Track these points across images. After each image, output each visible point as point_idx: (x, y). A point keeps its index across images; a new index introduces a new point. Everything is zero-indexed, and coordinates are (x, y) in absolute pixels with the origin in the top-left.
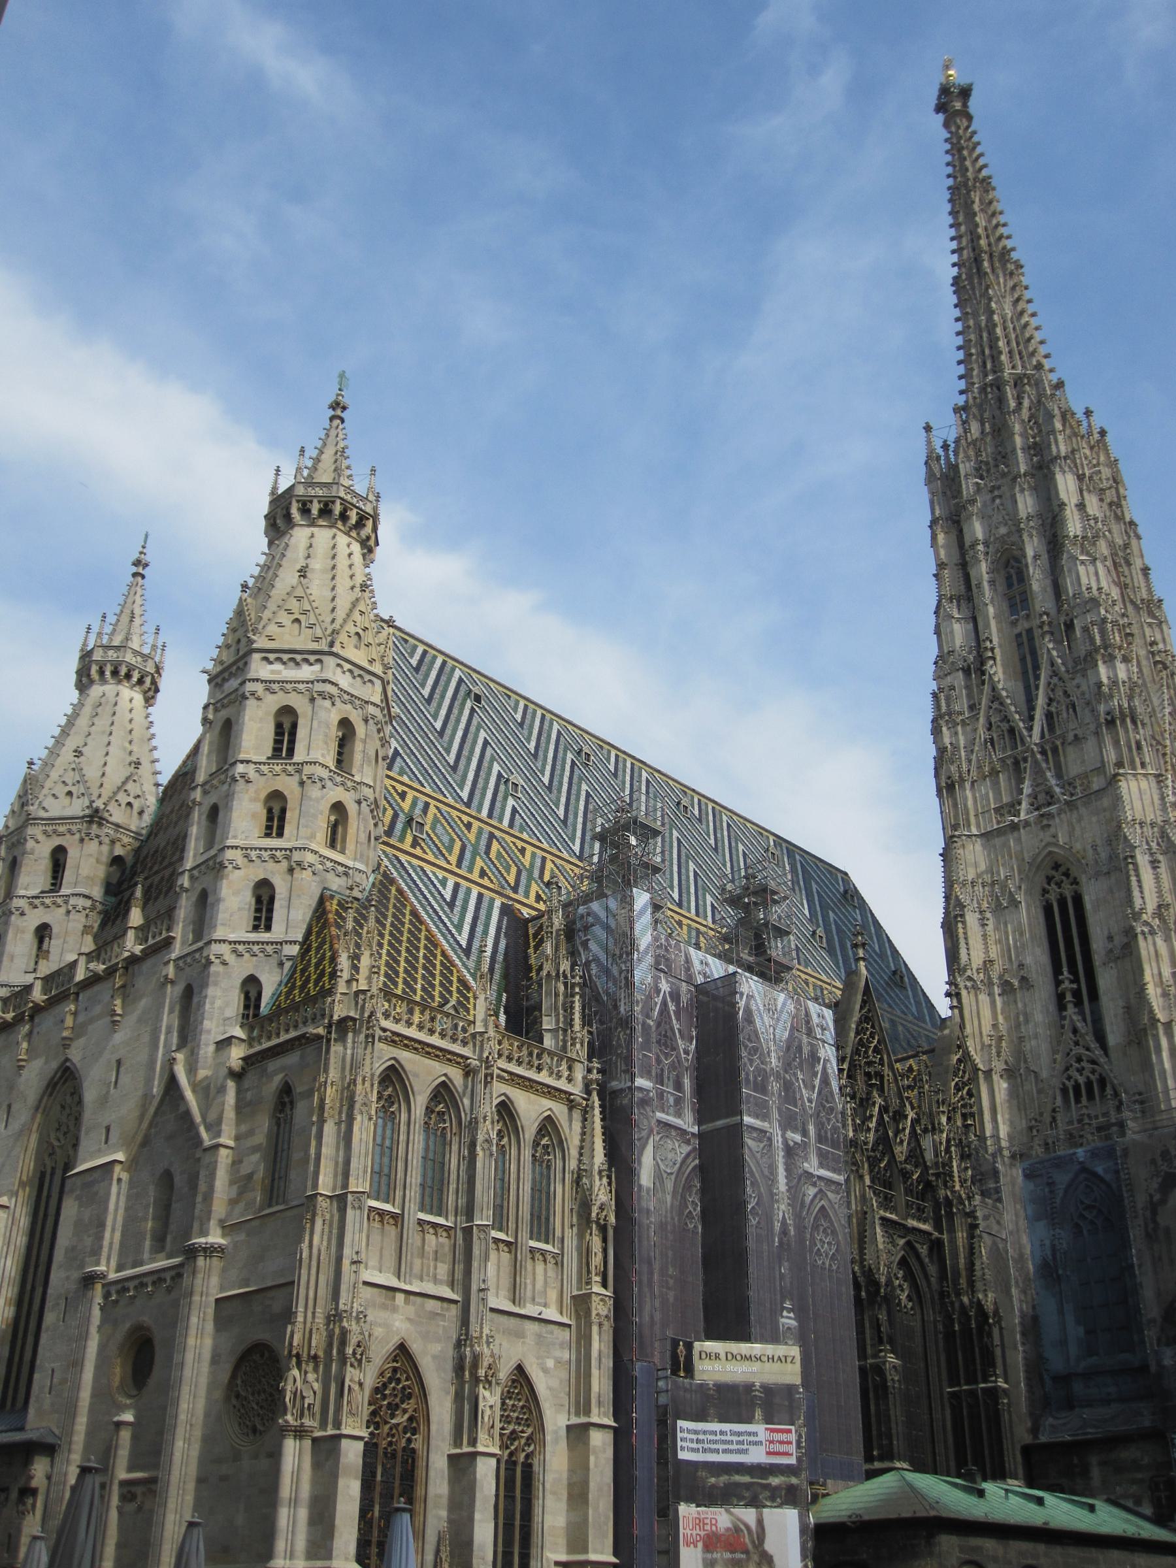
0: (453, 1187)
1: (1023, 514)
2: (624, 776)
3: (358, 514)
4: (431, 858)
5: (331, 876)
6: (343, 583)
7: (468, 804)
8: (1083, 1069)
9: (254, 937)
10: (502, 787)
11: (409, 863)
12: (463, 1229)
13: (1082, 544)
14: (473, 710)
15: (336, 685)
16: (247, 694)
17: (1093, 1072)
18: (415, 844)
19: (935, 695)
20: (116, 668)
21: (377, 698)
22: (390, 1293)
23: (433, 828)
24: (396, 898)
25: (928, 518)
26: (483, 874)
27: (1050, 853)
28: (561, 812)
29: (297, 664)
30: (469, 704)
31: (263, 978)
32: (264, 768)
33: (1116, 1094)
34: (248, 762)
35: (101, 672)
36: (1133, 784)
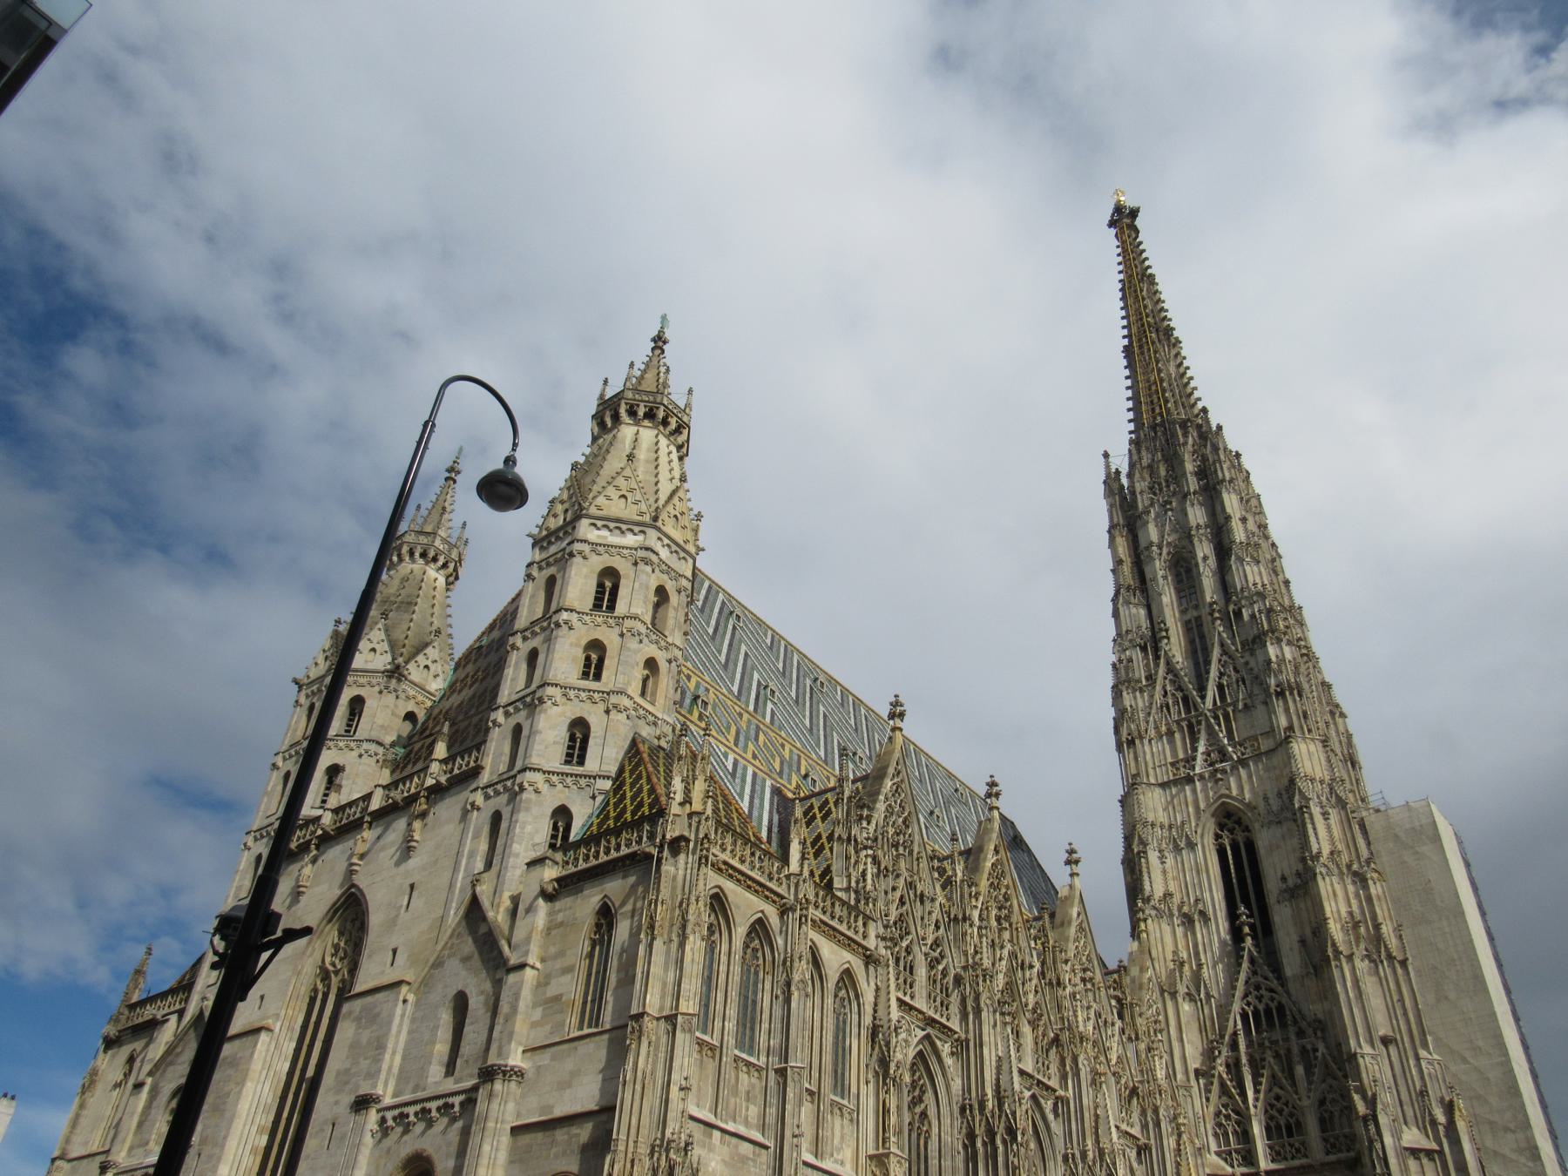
0: (765, 1026)
1: (1193, 523)
5: (642, 722)
6: (664, 475)
7: (738, 697)
9: (567, 769)
12: (777, 1071)
13: (1247, 550)
14: (734, 628)
15: (657, 554)
16: (575, 553)
17: (1272, 999)
19: (1114, 665)
20: (425, 551)
21: (689, 574)
22: (707, 1129)
23: (714, 709)
25: (1106, 525)
27: (1224, 803)
29: (623, 532)
30: (731, 622)
31: (574, 809)
33: (1295, 1022)
35: (411, 553)
36: (1303, 746)
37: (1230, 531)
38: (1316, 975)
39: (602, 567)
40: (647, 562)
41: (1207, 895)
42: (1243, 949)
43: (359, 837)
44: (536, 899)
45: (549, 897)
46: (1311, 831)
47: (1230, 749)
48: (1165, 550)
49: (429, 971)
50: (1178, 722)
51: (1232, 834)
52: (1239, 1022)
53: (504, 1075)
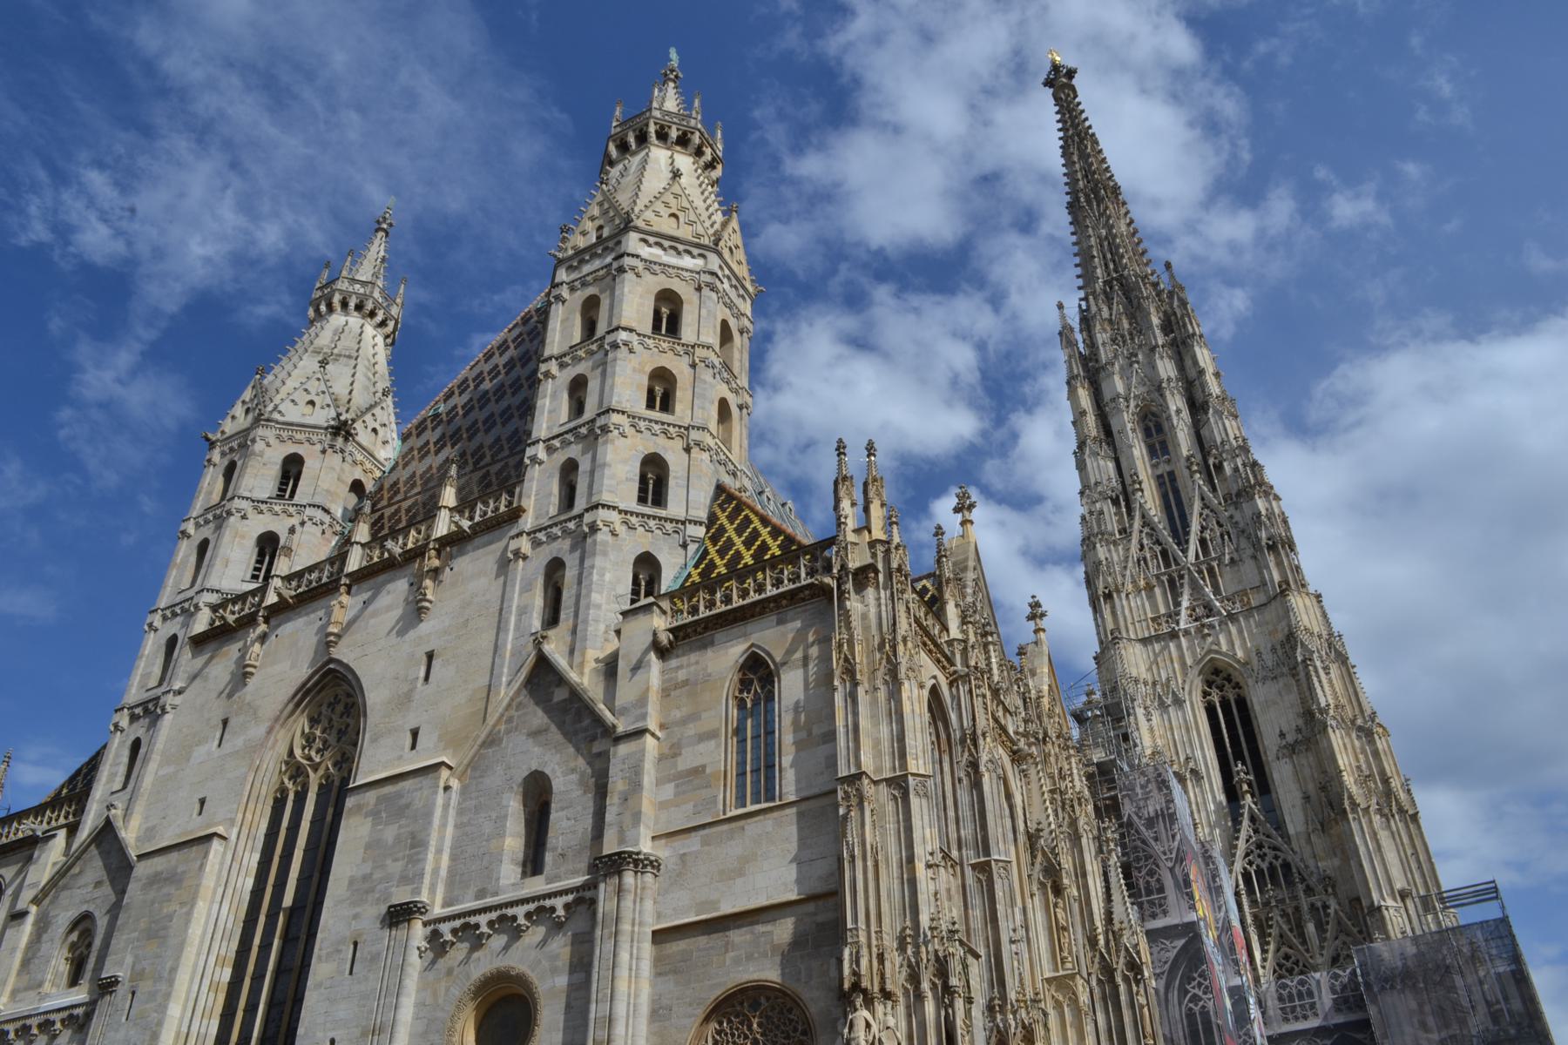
1: (1163, 375)
8: (1265, 854)
12: (974, 867)
19: (1083, 518)
20: (362, 302)
29: (679, 253)
31: (662, 558)
33: (1303, 880)
35: (344, 304)
36: (1299, 599)
37: (1203, 385)
38: (1323, 831)
41: (1198, 753)
42: (1243, 807)
43: (334, 602)
44: (646, 652)
45: (663, 652)
46: (1317, 684)
47: (1218, 604)
48: (1132, 404)
49: (479, 750)
50: (1158, 577)
51: (1221, 691)
52: (1241, 882)
53: (636, 866)
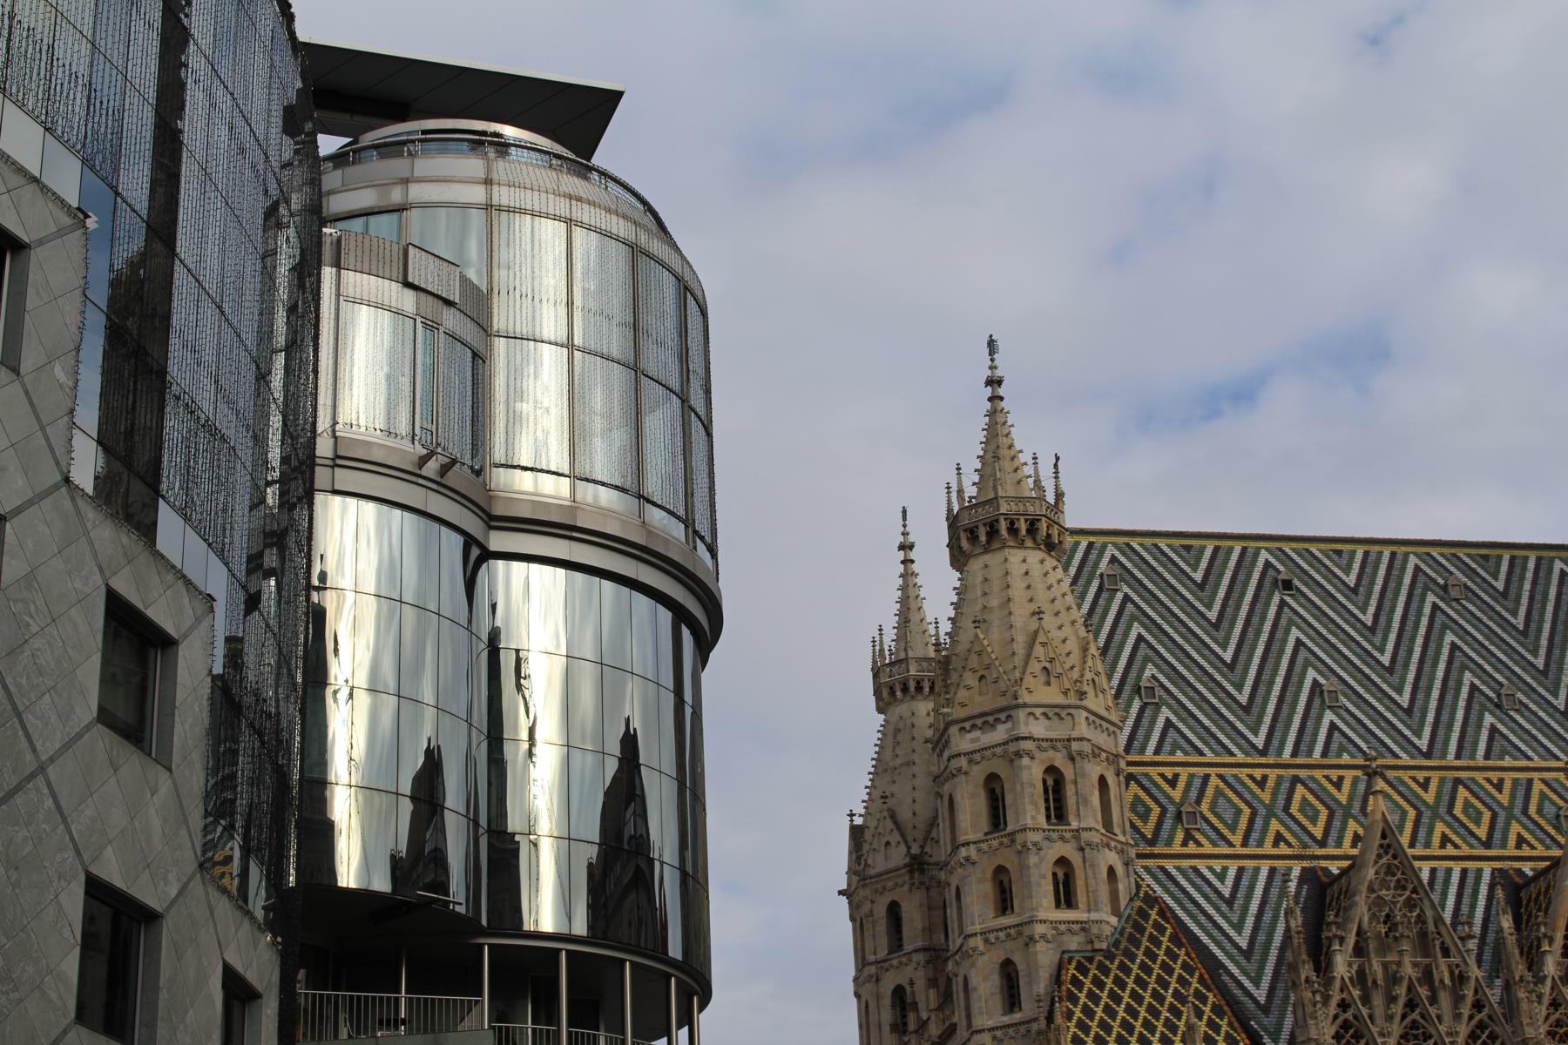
2: (1521, 587)
3: (1026, 520)
4: (1208, 849)
5: (1065, 938)
10: (1317, 702)
11: (1178, 868)
14: (1283, 603)
16: (954, 772)
18: (1188, 837)
20: (905, 684)
23: (1212, 809)
24: (1157, 925)
26: (1279, 838)
28: (1404, 700)
29: (992, 725)
30: (1276, 599)
32: (984, 846)
34: (968, 844)
35: (892, 692)
39: (983, 778)
40: (1018, 755)
